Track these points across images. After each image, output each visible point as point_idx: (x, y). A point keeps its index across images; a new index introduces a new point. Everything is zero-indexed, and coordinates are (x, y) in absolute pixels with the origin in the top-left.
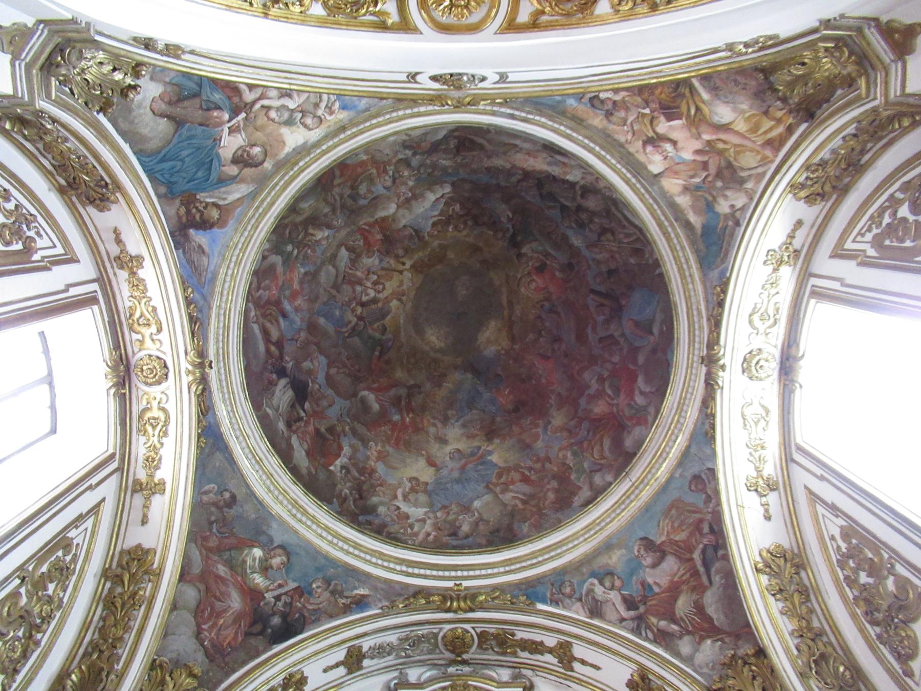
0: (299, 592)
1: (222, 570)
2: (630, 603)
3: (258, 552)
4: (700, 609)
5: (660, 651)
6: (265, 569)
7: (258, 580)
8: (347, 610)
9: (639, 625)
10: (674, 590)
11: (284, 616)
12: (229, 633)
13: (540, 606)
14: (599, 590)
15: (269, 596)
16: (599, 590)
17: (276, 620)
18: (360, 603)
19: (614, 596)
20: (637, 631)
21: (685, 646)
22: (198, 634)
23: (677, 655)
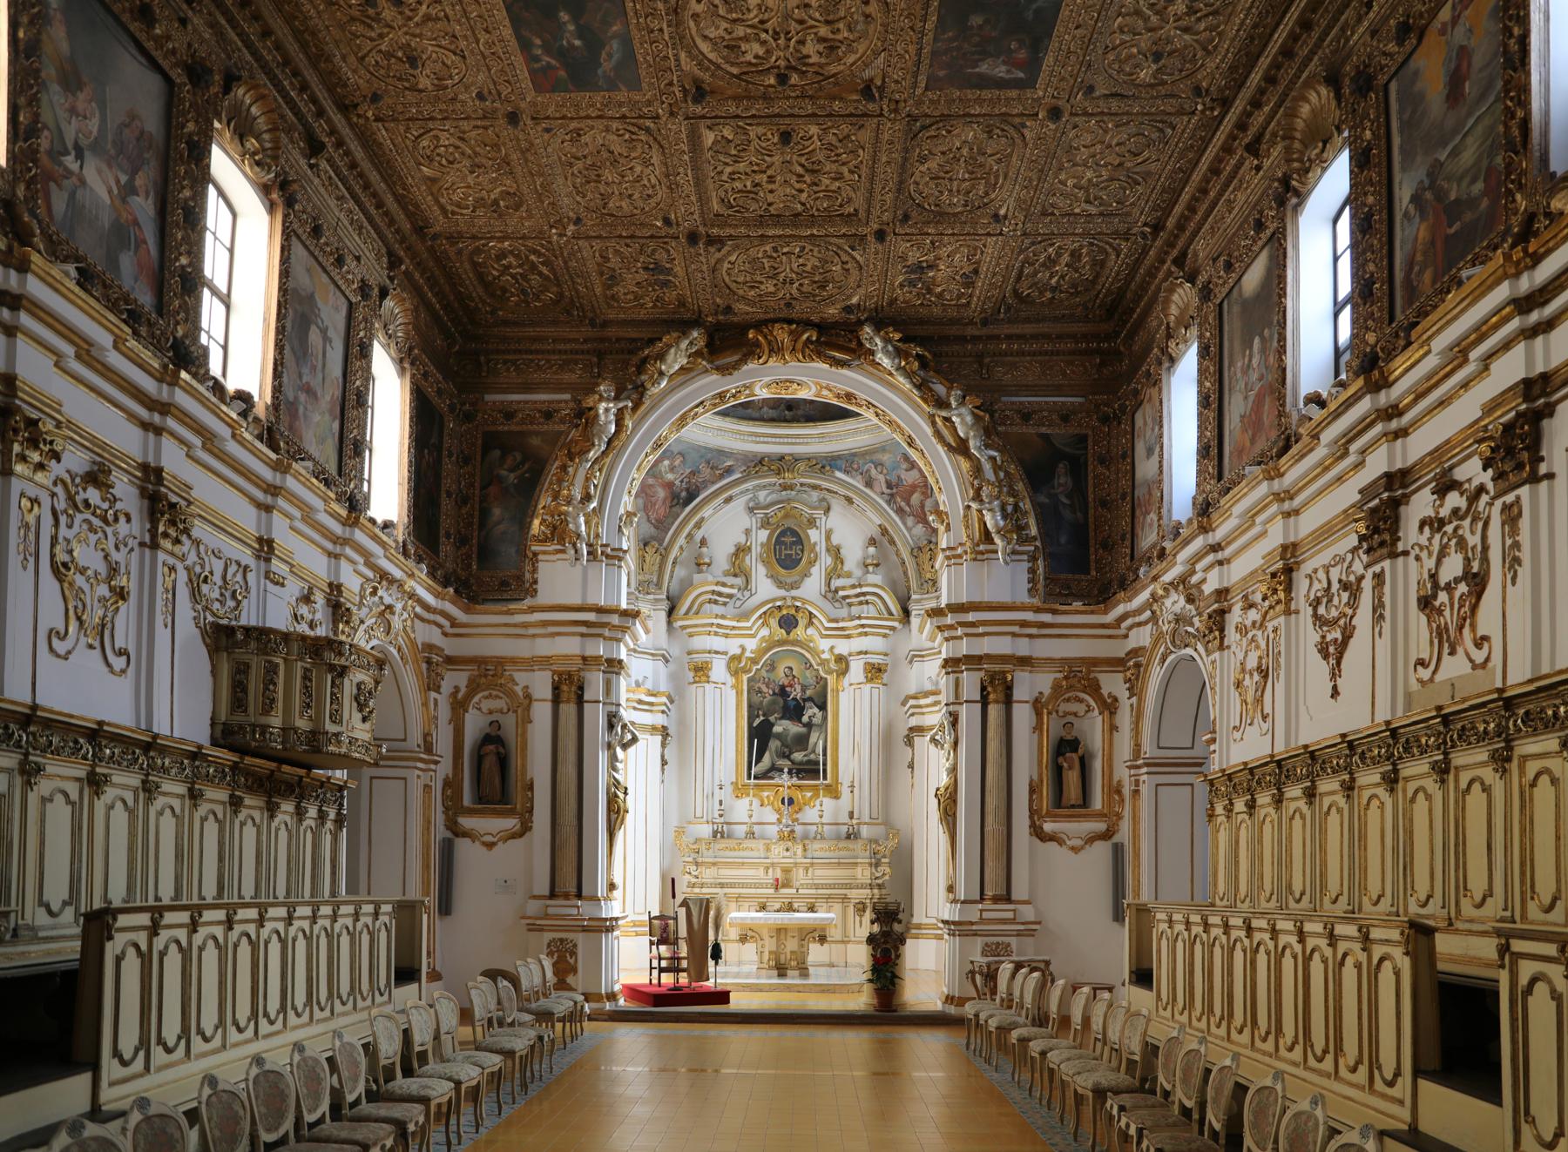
0: (693, 473)
1: (651, 481)
2: (889, 486)
3: (666, 463)
4: (922, 506)
5: (897, 519)
6: (672, 469)
7: (670, 476)
8: (722, 477)
9: (891, 499)
10: (914, 488)
11: (687, 490)
12: (662, 511)
13: (838, 474)
14: (873, 472)
15: (677, 482)
16: (873, 472)
17: (684, 494)
18: (729, 471)
19: (881, 478)
20: (888, 503)
21: (910, 521)
22: (649, 520)
23: (905, 524)
